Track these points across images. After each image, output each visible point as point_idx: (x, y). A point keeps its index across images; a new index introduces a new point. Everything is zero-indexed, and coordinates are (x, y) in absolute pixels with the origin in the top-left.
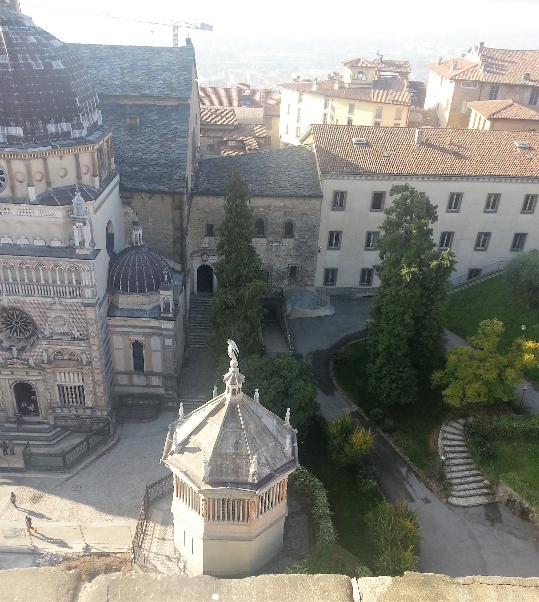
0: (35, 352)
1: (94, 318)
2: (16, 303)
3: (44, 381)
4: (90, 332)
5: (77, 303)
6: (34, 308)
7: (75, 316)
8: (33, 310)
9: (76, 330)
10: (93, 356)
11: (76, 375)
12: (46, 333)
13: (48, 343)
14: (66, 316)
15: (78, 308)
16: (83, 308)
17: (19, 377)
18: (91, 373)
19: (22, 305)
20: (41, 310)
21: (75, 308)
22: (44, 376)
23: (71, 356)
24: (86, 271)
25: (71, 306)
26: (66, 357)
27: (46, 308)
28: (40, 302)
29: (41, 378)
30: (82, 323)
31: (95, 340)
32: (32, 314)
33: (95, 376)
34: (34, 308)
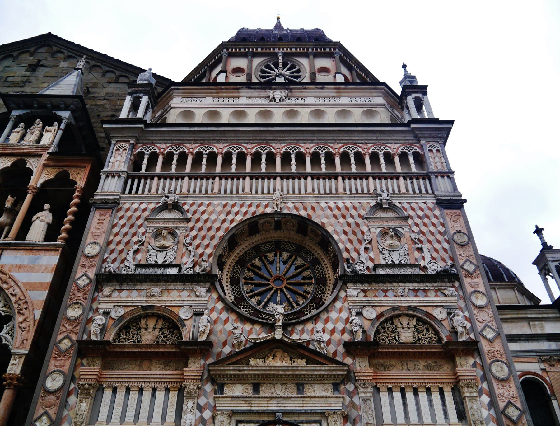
0: (327, 321)
1: (466, 232)
2: (296, 209)
3: (345, 418)
4: (461, 262)
5: (425, 203)
6: (335, 217)
7: (424, 229)
8: (333, 220)
9: (428, 258)
10: (480, 327)
11: (436, 396)
12: (358, 267)
13: (362, 294)
14: (403, 228)
15: (428, 212)
16: (437, 212)
17: (273, 406)
18: (484, 378)
19: (310, 212)
20: (350, 220)
21: (420, 213)
22: (348, 399)
23: (419, 332)
24: (434, 151)
25: (413, 209)
26: (407, 336)
27: (360, 216)
28: (349, 205)
29: (337, 406)
30: (439, 242)
31: (475, 280)
32: (329, 229)
33: (498, 389)
34: (335, 217)
